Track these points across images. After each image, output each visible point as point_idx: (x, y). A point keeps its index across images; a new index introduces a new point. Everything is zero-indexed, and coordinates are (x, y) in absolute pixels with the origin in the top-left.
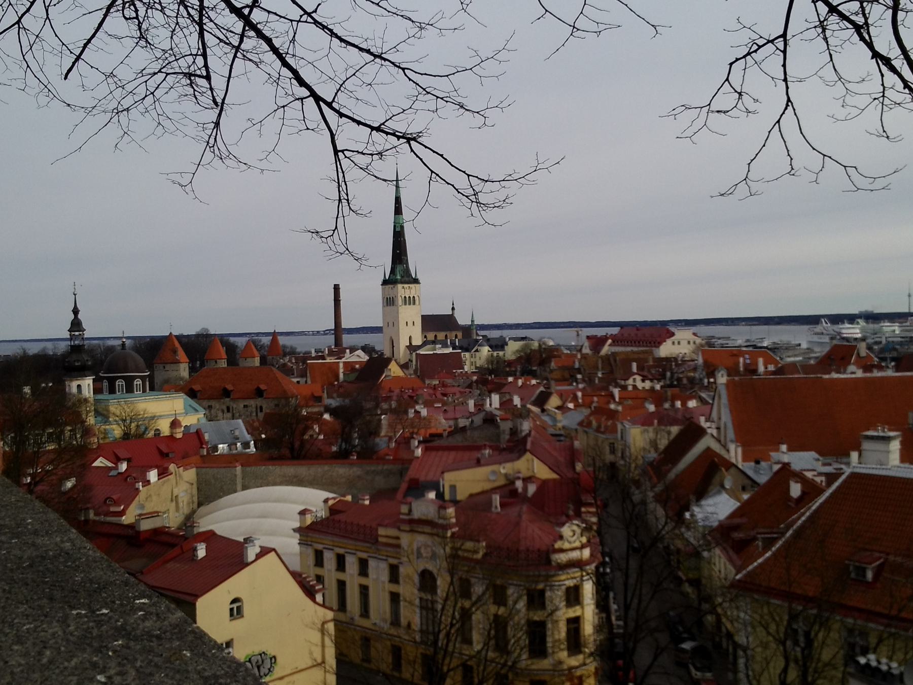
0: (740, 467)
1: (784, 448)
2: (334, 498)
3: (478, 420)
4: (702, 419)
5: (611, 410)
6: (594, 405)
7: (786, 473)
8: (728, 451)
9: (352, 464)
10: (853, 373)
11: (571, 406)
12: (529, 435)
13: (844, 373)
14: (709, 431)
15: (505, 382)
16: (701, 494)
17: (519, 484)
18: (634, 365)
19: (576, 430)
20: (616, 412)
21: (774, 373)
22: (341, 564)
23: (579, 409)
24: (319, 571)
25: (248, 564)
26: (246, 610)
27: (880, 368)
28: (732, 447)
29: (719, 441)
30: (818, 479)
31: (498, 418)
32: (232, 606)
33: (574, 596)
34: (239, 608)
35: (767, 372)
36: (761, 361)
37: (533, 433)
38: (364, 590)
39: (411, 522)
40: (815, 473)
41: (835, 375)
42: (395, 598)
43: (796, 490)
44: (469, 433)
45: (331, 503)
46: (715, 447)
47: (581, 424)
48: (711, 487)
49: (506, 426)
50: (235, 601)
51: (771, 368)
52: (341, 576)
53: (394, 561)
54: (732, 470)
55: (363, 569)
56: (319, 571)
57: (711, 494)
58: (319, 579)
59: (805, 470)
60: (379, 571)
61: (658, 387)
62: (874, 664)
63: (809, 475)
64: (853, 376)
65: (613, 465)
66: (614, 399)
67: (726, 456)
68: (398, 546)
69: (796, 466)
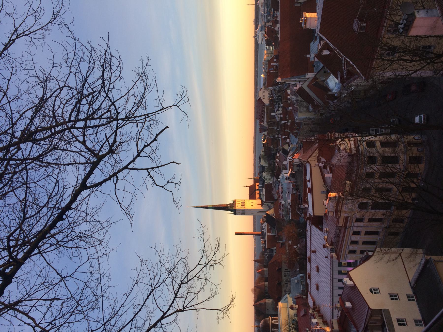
0: (316, 73)
3: (293, 180)
4: (295, 88)
5: (290, 124)
6: (288, 130)
7: (319, 56)
8: (309, 78)
10: (278, 28)
11: (288, 140)
13: (278, 32)
14: (300, 86)
15: (277, 167)
16: (327, 89)
18: (272, 114)
20: (291, 122)
21: (277, 59)
22: (354, 243)
26: (376, 286)
27: (277, 17)
28: (307, 77)
29: (305, 81)
30: (322, 43)
33: (371, 144)
34: (374, 290)
35: (277, 62)
36: (272, 64)
38: (367, 233)
39: (336, 212)
40: (319, 44)
41: (279, 36)
42: (371, 220)
43: (326, 53)
44: (298, 184)
46: (307, 83)
47: (296, 137)
48: (325, 86)
50: (371, 291)
51: (275, 60)
52: (361, 243)
53: (354, 220)
54: (317, 76)
55: (357, 233)
56: (358, 252)
57: (327, 85)
58: (362, 252)
59: (318, 48)
60: (358, 226)
61: (282, 105)
62: (403, 26)
63: (320, 47)
64: (280, 28)
65: (314, 124)
68: (347, 218)
69: (317, 52)
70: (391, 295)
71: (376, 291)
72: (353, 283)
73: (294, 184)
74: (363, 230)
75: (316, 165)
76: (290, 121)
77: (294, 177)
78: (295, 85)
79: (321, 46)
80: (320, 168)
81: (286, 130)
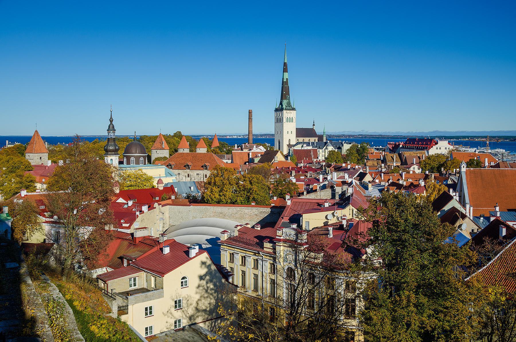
2: (241, 226)
9: (253, 206)
12: (352, 195)
14: (455, 197)
24: (232, 265)
25: (191, 259)
28: (468, 206)
31: (335, 186)
32: (182, 281)
36: (486, 159)
37: (354, 195)
45: (239, 228)
46: (458, 206)
50: (183, 278)
51: (493, 164)
52: (244, 268)
56: (232, 265)
67: (464, 212)
71: (184, 284)
78: (455, 190)
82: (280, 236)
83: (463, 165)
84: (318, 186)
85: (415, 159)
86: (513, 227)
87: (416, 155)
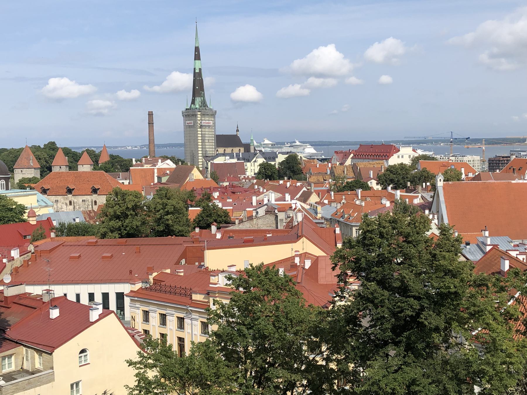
1: (487, 233)
6: (343, 201)
13: (524, 179)
15: (277, 184)
17: (297, 260)
19: (331, 219)
21: (473, 179)
23: (333, 204)
30: (521, 257)
35: (468, 178)
36: (463, 170)
40: (518, 252)
49: (281, 216)
50: (83, 351)
51: (471, 175)
63: (513, 254)
66: (358, 197)
69: (503, 247)
70: (77, 384)
72: (93, 321)
73: (254, 214)
74: (185, 335)
75: (296, 251)
76: (363, 204)
77: (266, 214)
79: (515, 256)
80: (293, 258)
81: (344, 197)
82: (216, 284)
83: (440, 178)
84: (254, 211)
85: (372, 172)
86: (517, 257)
87: (372, 166)
